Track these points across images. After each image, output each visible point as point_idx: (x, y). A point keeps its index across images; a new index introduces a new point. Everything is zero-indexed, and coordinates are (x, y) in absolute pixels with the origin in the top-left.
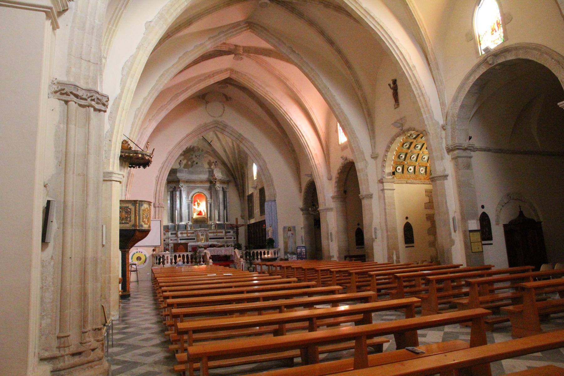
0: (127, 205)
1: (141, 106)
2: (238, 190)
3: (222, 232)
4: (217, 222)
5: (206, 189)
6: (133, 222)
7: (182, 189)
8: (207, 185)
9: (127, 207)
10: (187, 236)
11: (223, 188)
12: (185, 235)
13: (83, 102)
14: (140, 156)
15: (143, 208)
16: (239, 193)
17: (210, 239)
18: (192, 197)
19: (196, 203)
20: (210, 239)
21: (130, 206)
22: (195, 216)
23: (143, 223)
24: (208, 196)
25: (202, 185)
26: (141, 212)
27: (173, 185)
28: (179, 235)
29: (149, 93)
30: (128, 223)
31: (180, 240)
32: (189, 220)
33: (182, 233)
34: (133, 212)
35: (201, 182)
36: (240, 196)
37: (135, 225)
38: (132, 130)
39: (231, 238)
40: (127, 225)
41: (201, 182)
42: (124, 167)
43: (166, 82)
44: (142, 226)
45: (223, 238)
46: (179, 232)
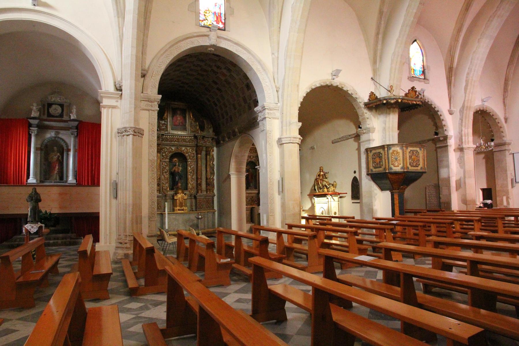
0: (378, 151)
1: (395, 50)
6: (383, 167)
9: (379, 153)
13: (122, 135)
14: (385, 102)
15: (391, 151)
21: (381, 151)
23: (392, 166)
26: (390, 155)
29: (400, 33)
30: (381, 167)
34: (383, 157)
37: (385, 169)
38: (390, 77)
40: (381, 169)
42: (389, 114)
43: (415, 11)
44: (391, 169)
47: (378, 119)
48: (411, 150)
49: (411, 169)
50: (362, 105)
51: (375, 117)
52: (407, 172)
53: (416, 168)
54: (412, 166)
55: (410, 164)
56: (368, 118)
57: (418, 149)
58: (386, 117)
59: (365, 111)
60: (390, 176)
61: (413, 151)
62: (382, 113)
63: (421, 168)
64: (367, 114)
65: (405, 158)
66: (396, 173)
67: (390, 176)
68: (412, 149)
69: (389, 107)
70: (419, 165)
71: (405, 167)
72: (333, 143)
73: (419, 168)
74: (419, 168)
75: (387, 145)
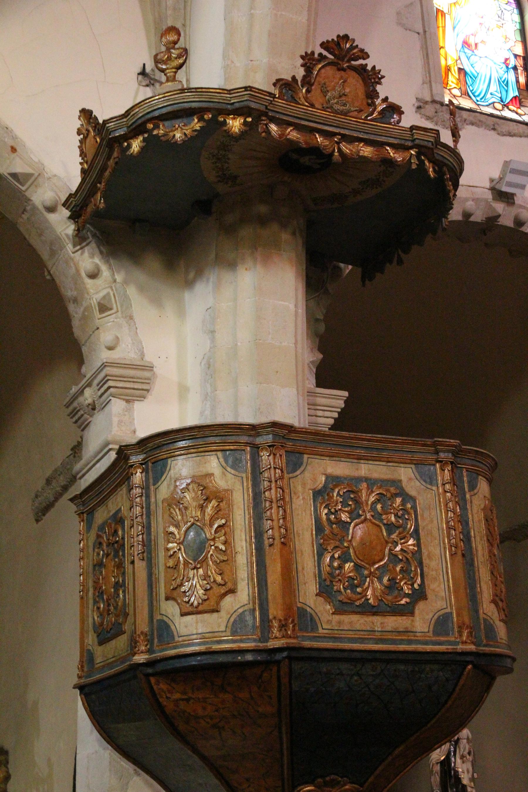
14: (136, 145)
23: (170, 610)
42: (232, 265)
44: (163, 631)
47: (181, 312)
48: (334, 481)
49: (335, 627)
50: (62, 225)
51: (157, 302)
52: (295, 654)
53: (392, 622)
54: (343, 608)
55: (325, 591)
56: (103, 308)
57: (406, 474)
58: (217, 287)
59: (87, 259)
60: (170, 695)
61: (351, 488)
62: (200, 273)
63: (442, 624)
64: (90, 275)
65: (271, 530)
66: (213, 670)
67: (170, 695)
68: (341, 468)
69: (230, 219)
70: (420, 595)
71: (275, 610)
72: (37, 521)
73: (421, 622)
74: (421, 622)
75: (143, 443)
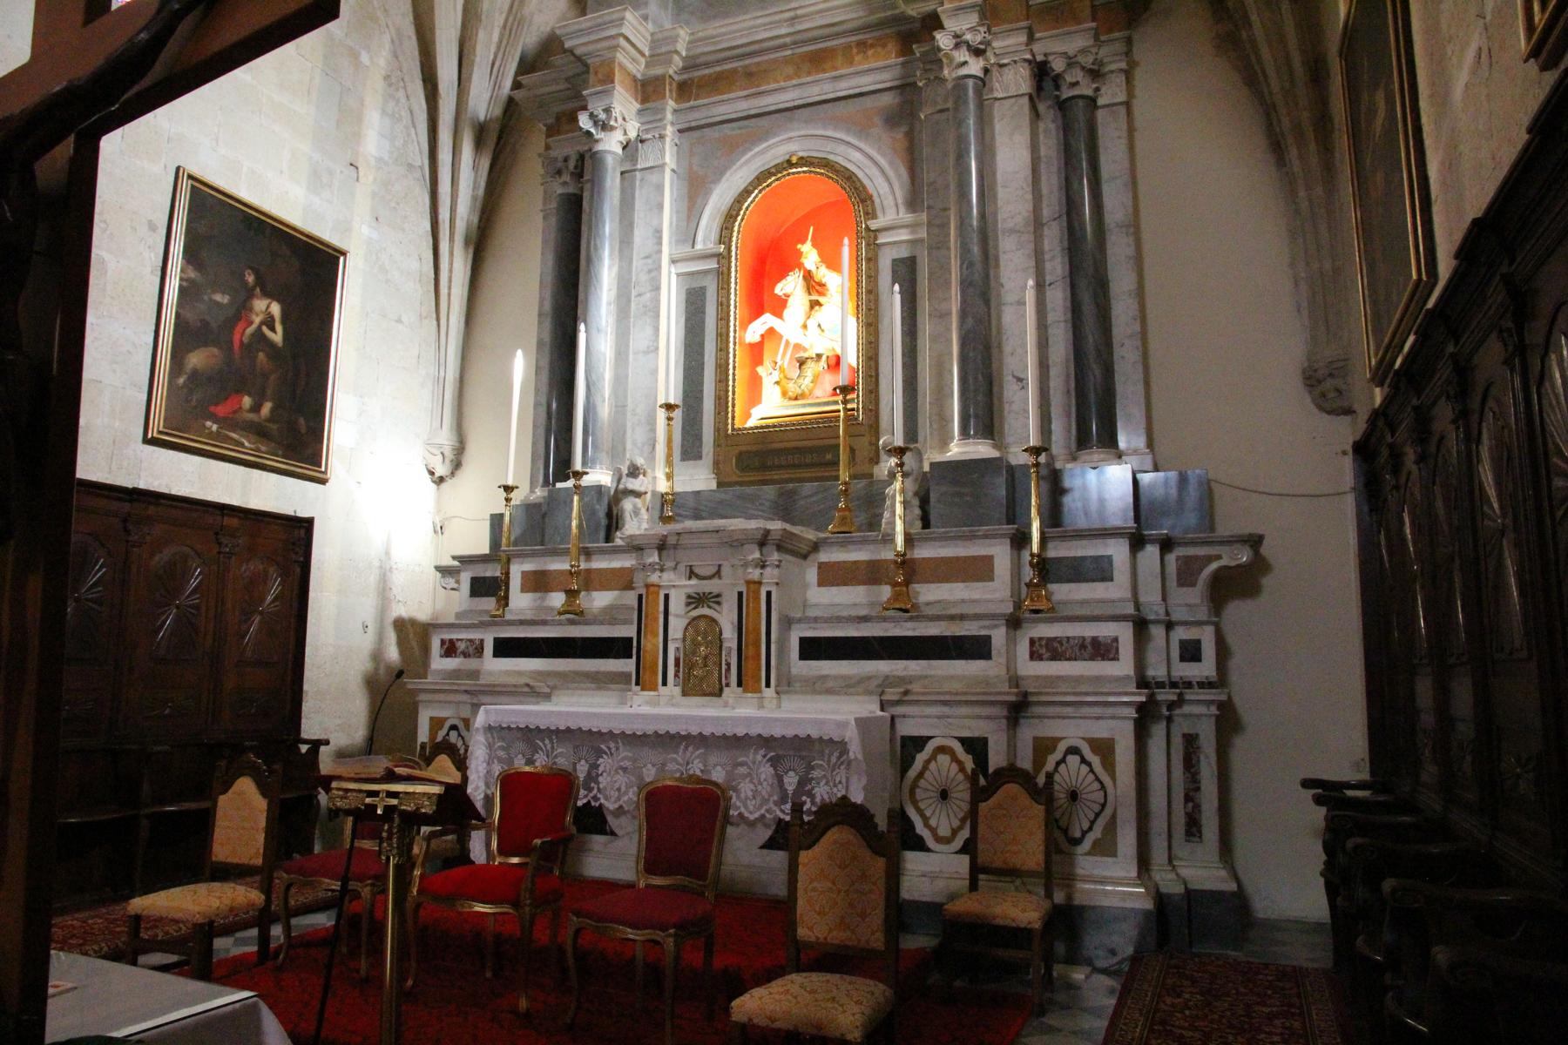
2: (1252, 79)
3: (979, 570)
4: (957, 450)
5: (862, 130)
7: (611, 144)
8: (876, 73)
10: (574, 613)
11: (1041, 72)
12: (557, 599)
16: (1268, 111)
17: (813, 649)
18: (730, 217)
19: (791, 286)
20: (813, 649)
22: (769, 405)
24: (883, 178)
25: (819, 87)
27: (565, 148)
28: (521, 601)
31: (506, 648)
32: (691, 451)
33: (538, 583)
35: (816, 56)
36: (1277, 147)
39: (1102, 650)
41: (816, 56)
45: (976, 648)
46: (517, 570)
